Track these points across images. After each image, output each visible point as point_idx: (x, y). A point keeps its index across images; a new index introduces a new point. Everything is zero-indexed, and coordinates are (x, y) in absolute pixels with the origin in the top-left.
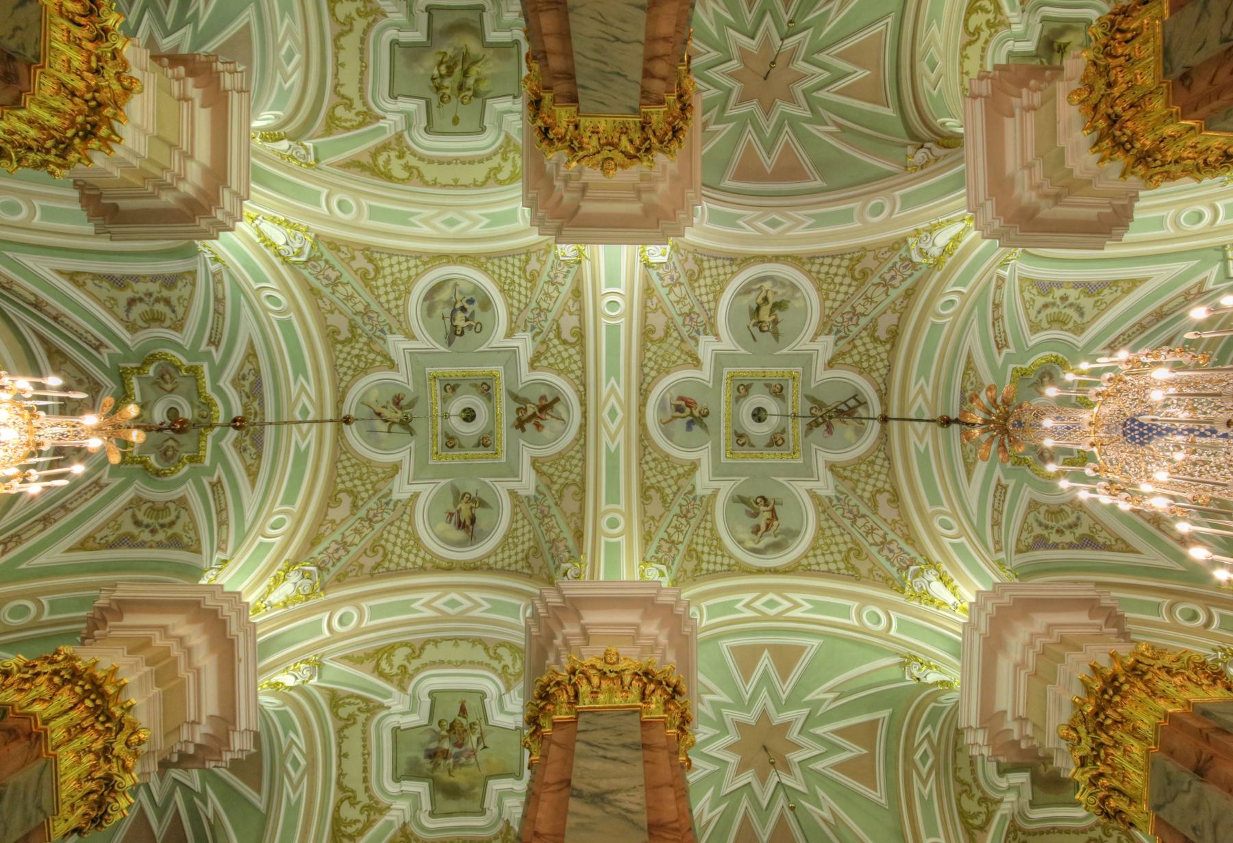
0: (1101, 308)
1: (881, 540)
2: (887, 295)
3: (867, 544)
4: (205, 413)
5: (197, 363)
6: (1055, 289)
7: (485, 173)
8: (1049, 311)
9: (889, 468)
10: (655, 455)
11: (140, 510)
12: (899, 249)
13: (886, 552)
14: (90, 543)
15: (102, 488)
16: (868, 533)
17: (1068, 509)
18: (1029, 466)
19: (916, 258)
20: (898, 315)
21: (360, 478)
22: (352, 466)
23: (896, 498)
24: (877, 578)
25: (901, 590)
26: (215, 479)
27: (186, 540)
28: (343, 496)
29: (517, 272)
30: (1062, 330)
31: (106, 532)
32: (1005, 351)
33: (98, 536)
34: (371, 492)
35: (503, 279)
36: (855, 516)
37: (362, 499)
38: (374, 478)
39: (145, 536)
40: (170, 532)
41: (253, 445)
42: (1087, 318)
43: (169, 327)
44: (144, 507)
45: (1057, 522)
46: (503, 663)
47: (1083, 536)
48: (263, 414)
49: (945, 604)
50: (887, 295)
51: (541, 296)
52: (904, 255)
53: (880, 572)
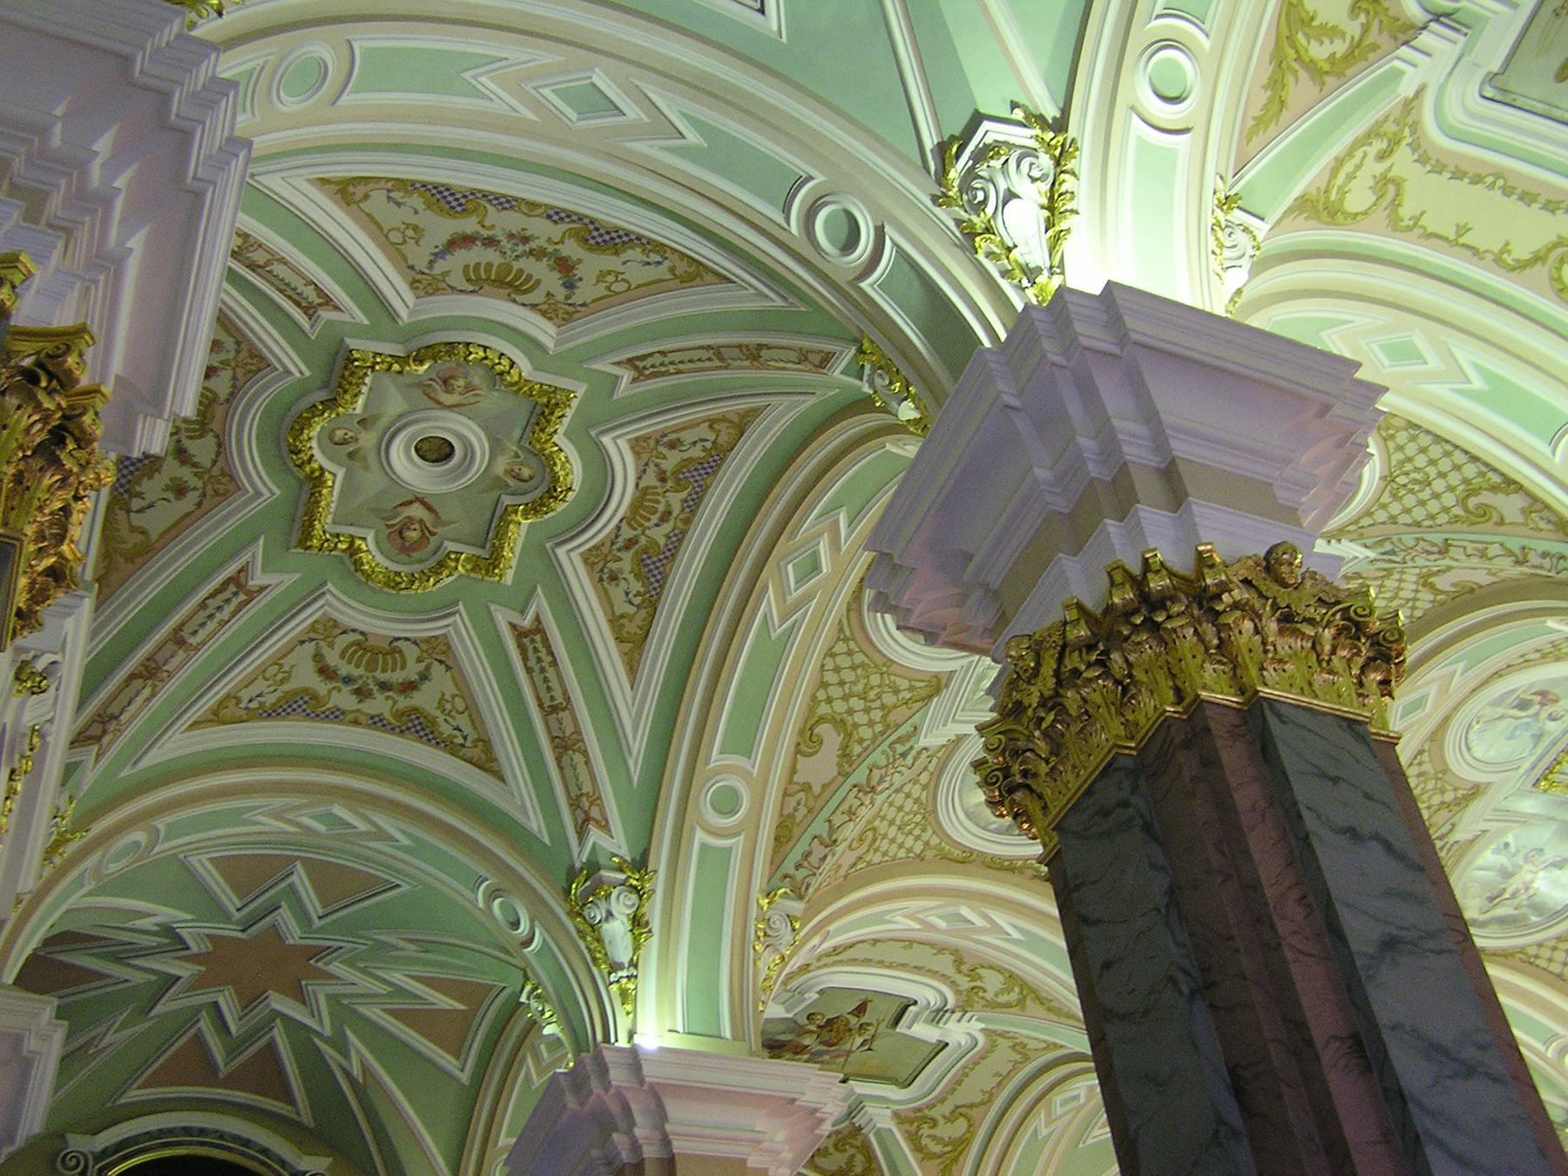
4: (526, 472)
5: (560, 382)
7: (1538, 242)
10: (1427, 767)
11: (331, 646)
14: (231, 710)
15: (251, 595)
21: (863, 696)
22: (854, 668)
26: (527, 622)
27: (446, 730)
28: (824, 730)
29: (1454, 478)
31: (260, 686)
33: (245, 695)
34: (879, 728)
35: (1408, 467)
37: (860, 741)
38: (889, 699)
39: (344, 699)
40: (403, 703)
41: (638, 577)
43: (534, 306)
44: (342, 641)
46: (978, 983)
48: (688, 521)
51: (1470, 546)
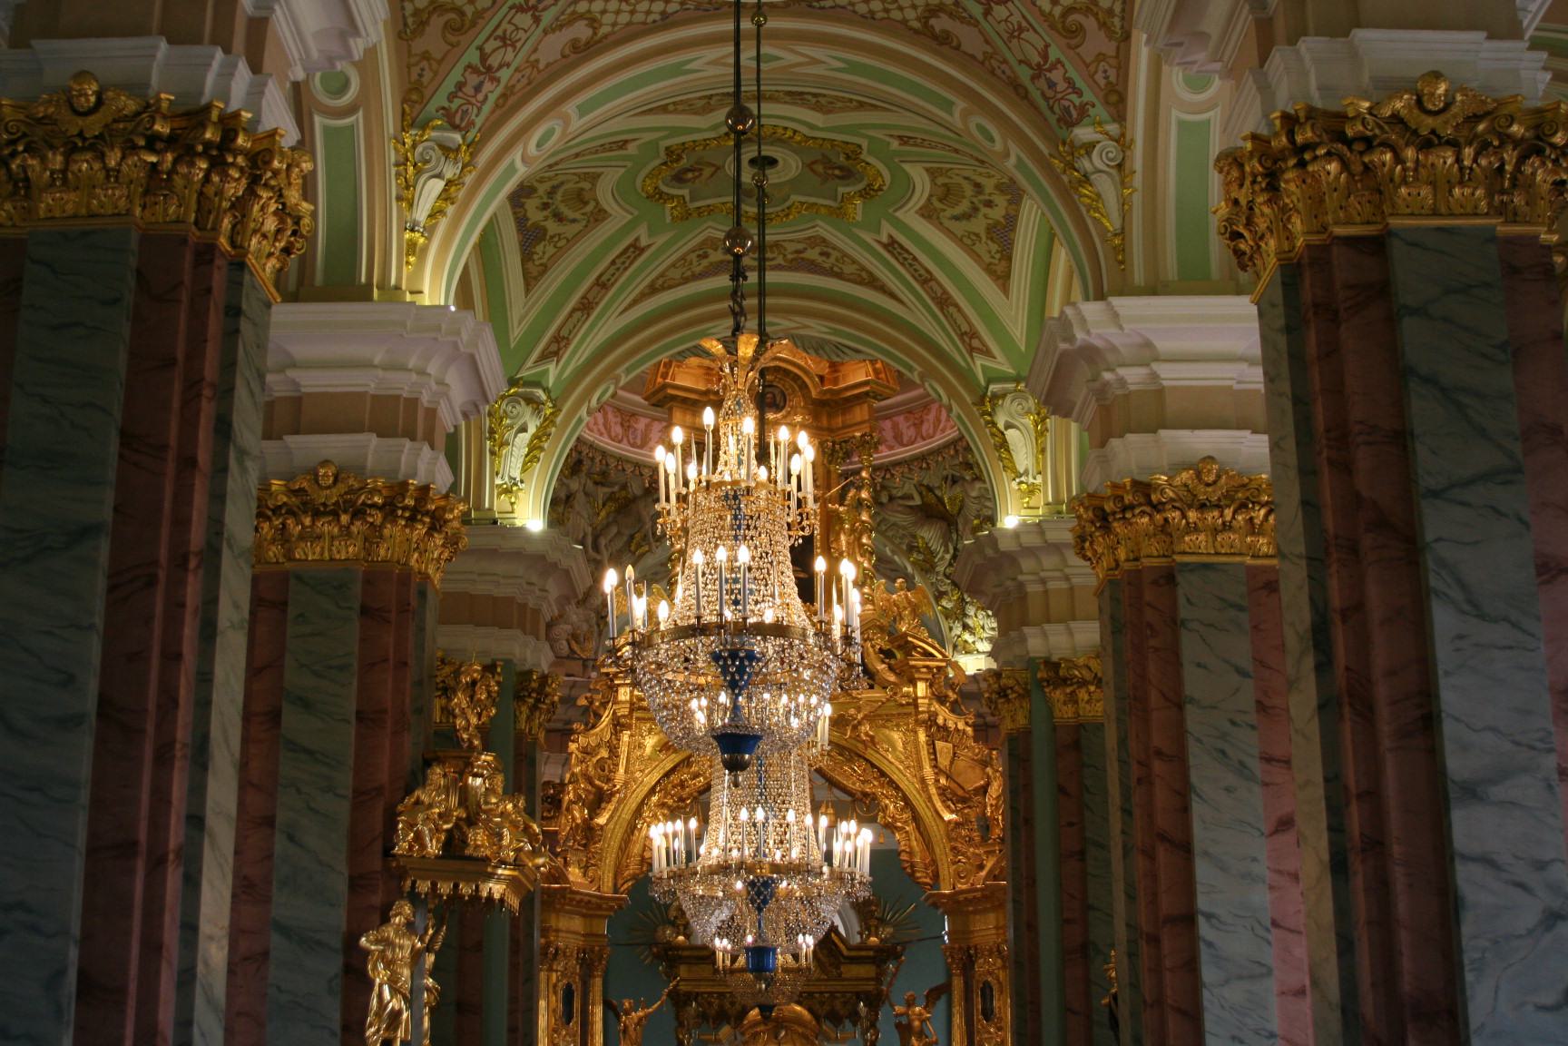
0: (965, 239)
1: (496, 65)
2: (1020, 62)
3: (478, 42)
6: (1008, 197)
8: (969, 190)
9: (644, 23)
12: (1107, 103)
13: (473, 80)
16: (503, 38)
17: (589, 208)
18: (665, 164)
19: (1083, 133)
20: (980, 57)
23: (582, 51)
24: (415, 71)
25: (411, 119)
30: (931, 196)
32: (895, 144)
36: (534, 8)
42: (947, 223)
45: (562, 201)
47: (545, 230)
49: (411, 205)
50: (1020, 62)
52: (1092, 111)
53: (428, 75)
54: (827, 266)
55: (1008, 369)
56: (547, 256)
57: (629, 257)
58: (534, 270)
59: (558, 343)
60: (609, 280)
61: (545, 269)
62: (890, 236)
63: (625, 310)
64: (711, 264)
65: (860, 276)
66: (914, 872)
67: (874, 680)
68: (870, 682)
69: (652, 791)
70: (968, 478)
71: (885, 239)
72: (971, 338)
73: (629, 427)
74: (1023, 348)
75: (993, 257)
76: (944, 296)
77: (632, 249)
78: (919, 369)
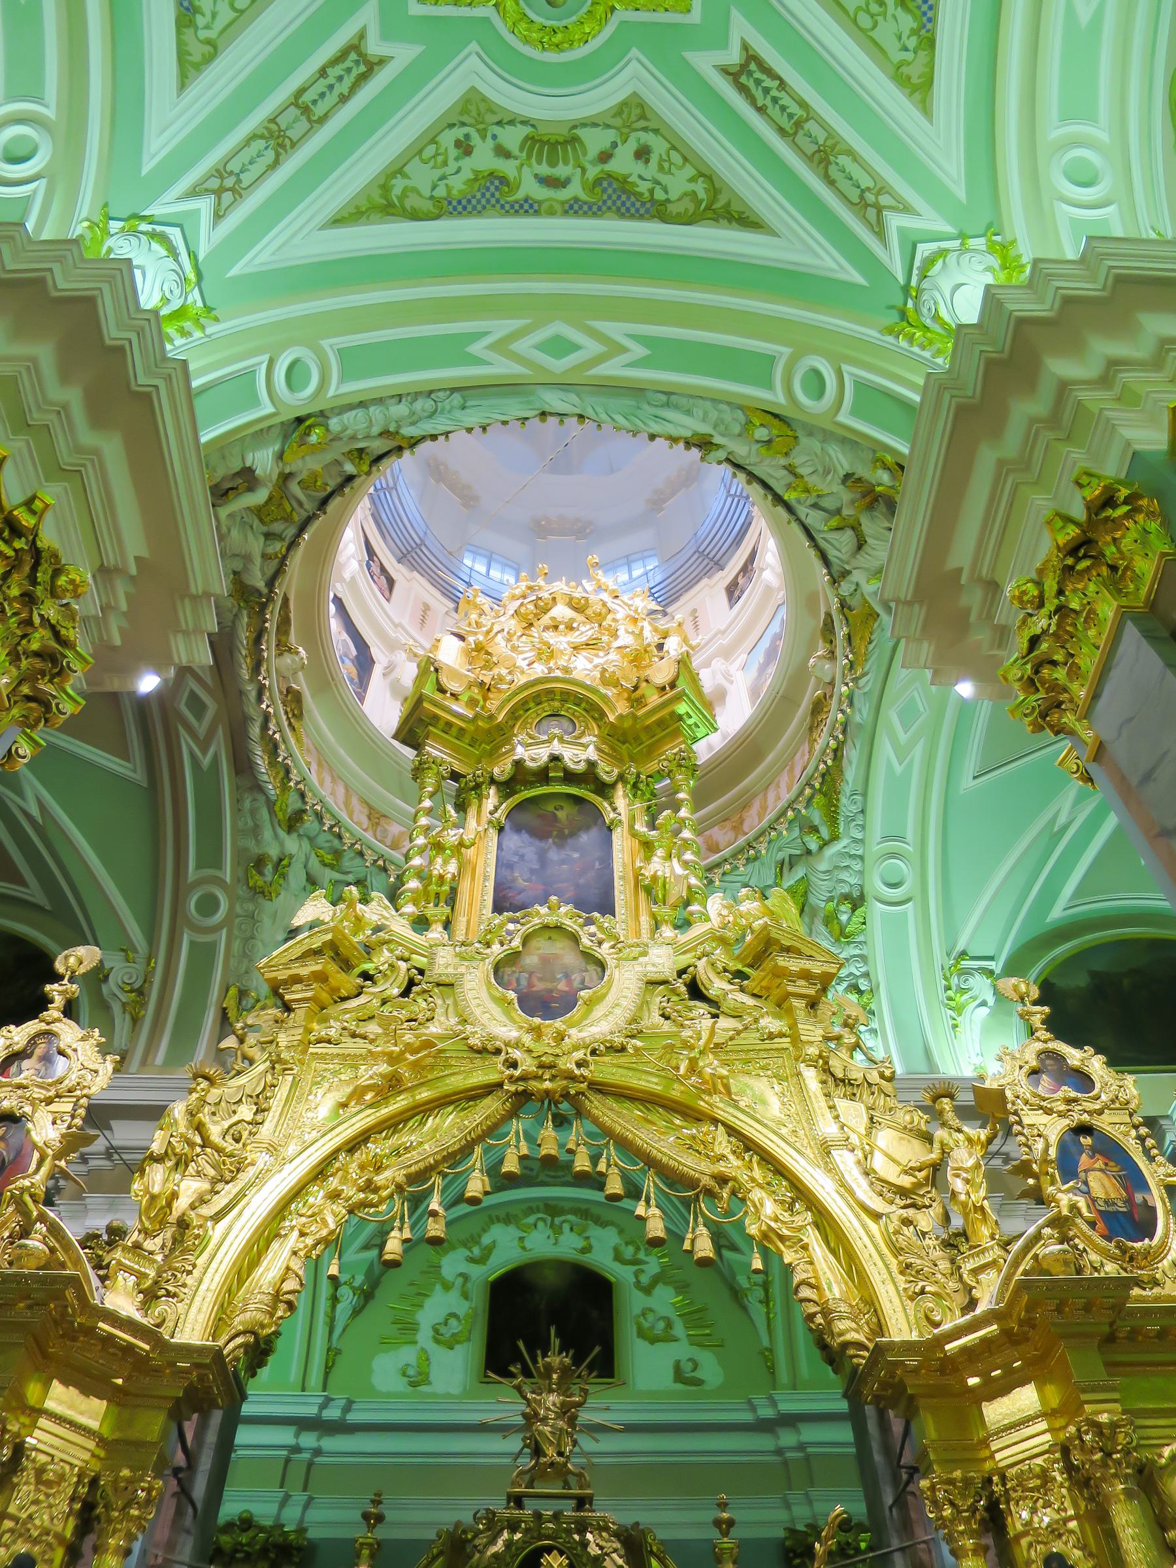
0: (865, 21)
54: (643, 187)
55: (949, 229)
56: (219, 24)
57: (349, 70)
58: (197, 51)
59: (222, 178)
60: (315, 102)
61: (214, 49)
62: (745, 47)
63: (337, 221)
64: (476, 172)
65: (694, 192)
66: (829, 1323)
67: (718, 1008)
68: (714, 1011)
69: (320, 1173)
70: (813, 846)
71: (734, 57)
72: (879, 193)
73: (378, 824)
74: (962, 195)
75: (906, 49)
76: (829, 143)
77: (353, 56)
78: (786, 351)
